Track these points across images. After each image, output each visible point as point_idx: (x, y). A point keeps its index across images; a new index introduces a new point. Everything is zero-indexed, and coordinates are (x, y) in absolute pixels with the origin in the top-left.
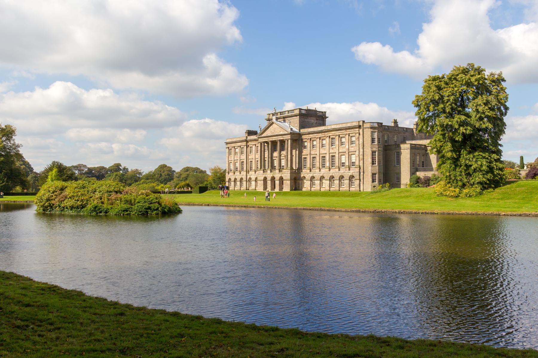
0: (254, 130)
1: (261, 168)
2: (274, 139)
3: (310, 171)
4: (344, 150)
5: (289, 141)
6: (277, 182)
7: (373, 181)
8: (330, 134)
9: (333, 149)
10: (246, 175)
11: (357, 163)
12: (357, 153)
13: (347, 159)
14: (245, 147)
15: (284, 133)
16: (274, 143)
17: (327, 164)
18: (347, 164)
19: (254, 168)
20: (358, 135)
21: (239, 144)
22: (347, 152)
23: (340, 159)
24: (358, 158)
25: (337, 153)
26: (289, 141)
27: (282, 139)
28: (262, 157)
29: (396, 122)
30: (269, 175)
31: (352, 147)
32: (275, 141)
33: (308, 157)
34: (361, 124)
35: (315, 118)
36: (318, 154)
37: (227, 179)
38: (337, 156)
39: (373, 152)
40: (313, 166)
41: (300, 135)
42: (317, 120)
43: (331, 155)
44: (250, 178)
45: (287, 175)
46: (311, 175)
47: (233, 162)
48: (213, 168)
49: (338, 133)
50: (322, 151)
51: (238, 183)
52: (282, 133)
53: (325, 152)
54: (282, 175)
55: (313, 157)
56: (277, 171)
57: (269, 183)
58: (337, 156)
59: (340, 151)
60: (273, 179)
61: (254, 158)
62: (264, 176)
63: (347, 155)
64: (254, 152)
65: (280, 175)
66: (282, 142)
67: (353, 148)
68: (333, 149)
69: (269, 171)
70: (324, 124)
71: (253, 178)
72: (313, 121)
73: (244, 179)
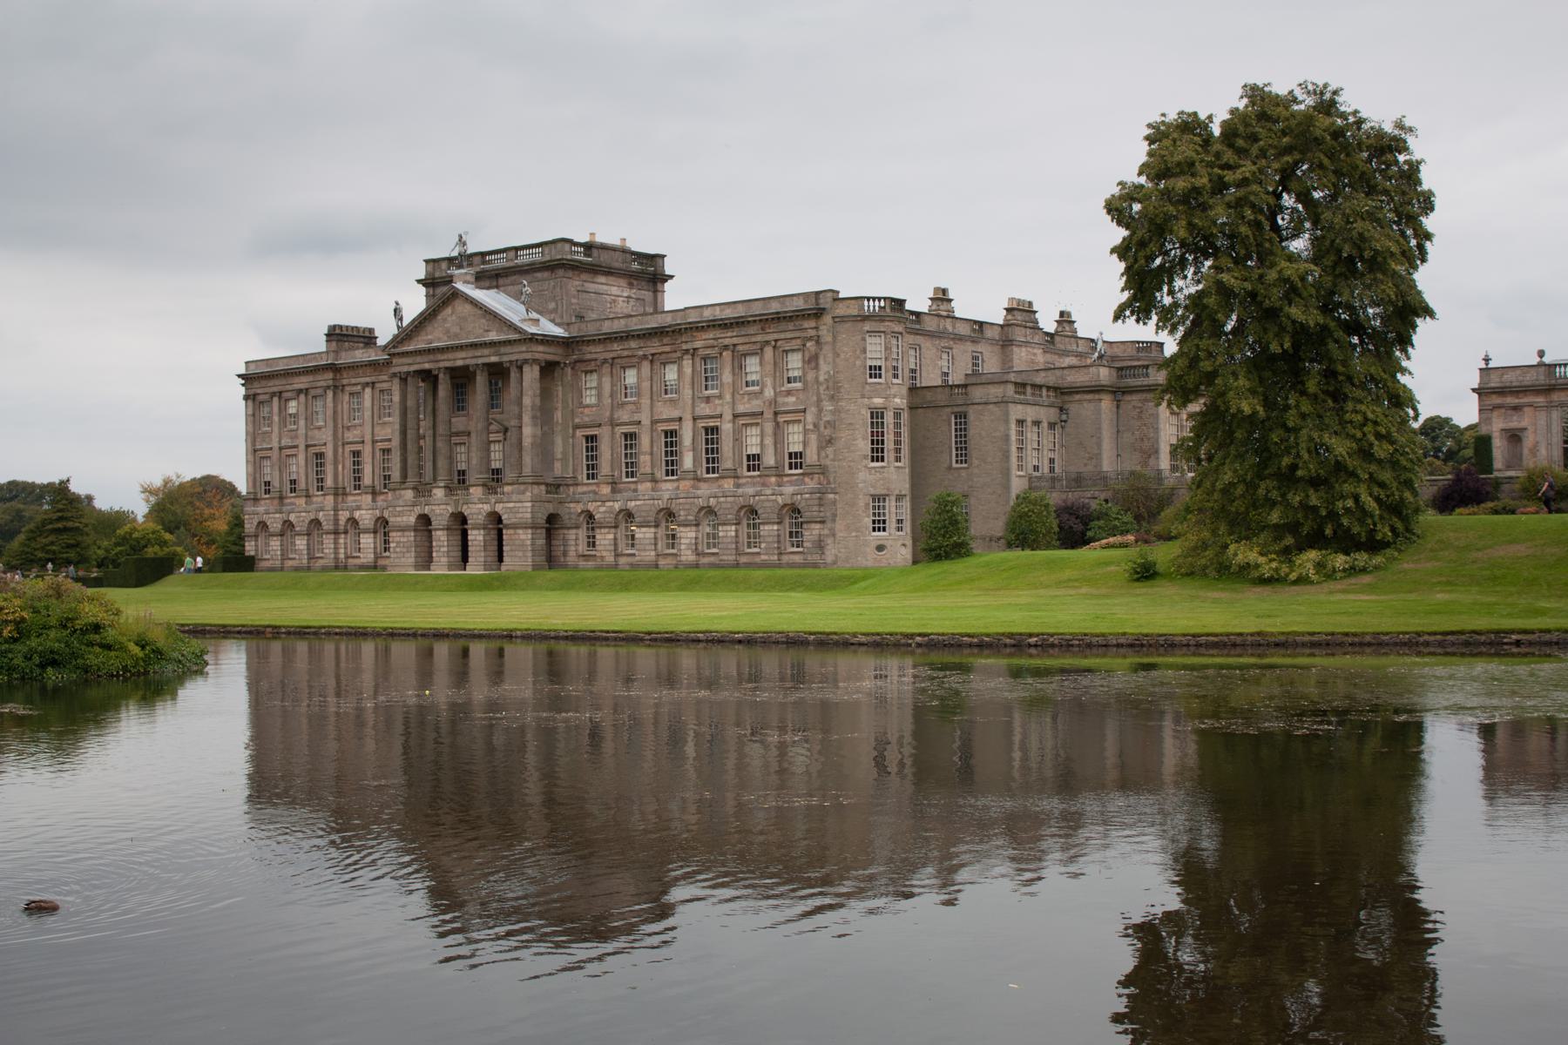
0: (362, 323)
1: (404, 476)
2: (459, 360)
3: (614, 491)
4: (755, 405)
5: (526, 369)
6: (476, 537)
7: (880, 525)
9: (708, 399)
10: (336, 510)
11: (811, 457)
12: (810, 418)
13: (769, 441)
14: (330, 394)
15: (503, 337)
16: (461, 379)
17: (688, 462)
18: (769, 460)
19: (367, 480)
21: (301, 382)
22: (768, 415)
23: (738, 440)
24: (813, 437)
25: (728, 416)
27: (494, 359)
28: (411, 434)
29: (941, 297)
30: (440, 506)
31: (789, 393)
32: (466, 367)
33: (604, 433)
34: (825, 302)
35: (623, 282)
36: (646, 422)
37: (250, 526)
39: (877, 415)
40: (632, 469)
41: (567, 344)
42: (631, 285)
43: (701, 424)
44: (353, 522)
45: (519, 506)
46: (617, 506)
47: (275, 454)
48: (158, 482)
49: (729, 337)
50: (666, 412)
51: (301, 543)
52: (493, 336)
53: (676, 414)
54: (499, 508)
55: (627, 436)
56: (476, 492)
57: (441, 539)
58: (727, 427)
59: (741, 409)
60: (460, 520)
61: (368, 438)
62: (418, 510)
63: (769, 427)
64: (368, 414)
65: (487, 508)
66: (498, 373)
67: (792, 399)
68: (708, 399)
69: (439, 493)
70: (657, 309)
71: (366, 517)
72: (615, 290)
73: (327, 526)
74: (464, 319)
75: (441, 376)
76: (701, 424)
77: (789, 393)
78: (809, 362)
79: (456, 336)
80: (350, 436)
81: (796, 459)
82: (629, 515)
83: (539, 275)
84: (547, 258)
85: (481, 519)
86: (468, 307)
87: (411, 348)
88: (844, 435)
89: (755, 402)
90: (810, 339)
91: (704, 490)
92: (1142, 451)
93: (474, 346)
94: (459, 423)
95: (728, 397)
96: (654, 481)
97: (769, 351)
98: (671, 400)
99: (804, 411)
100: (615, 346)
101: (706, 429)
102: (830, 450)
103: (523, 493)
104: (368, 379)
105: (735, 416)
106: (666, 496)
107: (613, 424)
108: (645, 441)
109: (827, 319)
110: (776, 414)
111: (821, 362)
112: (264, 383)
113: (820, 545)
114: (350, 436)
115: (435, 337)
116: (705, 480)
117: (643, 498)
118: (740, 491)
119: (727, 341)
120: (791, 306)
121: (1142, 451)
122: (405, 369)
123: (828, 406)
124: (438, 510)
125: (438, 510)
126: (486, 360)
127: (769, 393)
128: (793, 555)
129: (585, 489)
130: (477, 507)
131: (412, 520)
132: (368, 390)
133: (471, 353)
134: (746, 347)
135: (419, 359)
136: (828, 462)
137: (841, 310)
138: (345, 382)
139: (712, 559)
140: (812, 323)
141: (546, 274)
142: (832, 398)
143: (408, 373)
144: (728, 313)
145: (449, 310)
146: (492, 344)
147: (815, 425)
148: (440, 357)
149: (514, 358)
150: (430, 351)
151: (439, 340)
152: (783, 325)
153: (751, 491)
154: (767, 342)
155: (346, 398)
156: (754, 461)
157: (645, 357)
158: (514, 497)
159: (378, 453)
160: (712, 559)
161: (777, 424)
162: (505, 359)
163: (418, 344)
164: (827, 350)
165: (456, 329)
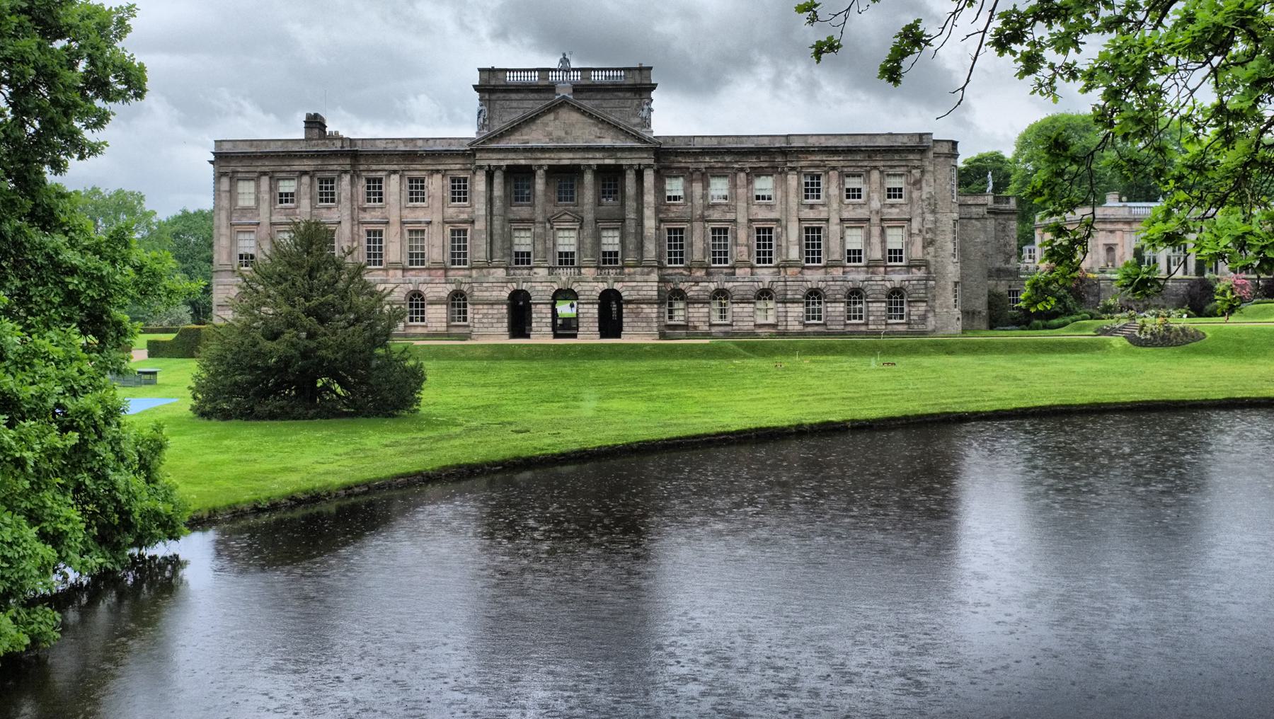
2: (566, 159)
3: (708, 274)
4: (861, 213)
9: (812, 206)
13: (876, 240)
14: (346, 178)
15: (618, 144)
20: (916, 173)
22: (875, 219)
24: (918, 241)
25: (835, 219)
26: (649, 178)
31: (892, 206)
36: (742, 219)
46: (713, 286)
47: (264, 230)
49: (834, 160)
52: (607, 142)
54: (617, 286)
59: (846, 215)
63: (876, 231)
65: (603, 286)
67: (895, 210)
68: (812, 206)
75: (540, 173)
76: (755, 225)
77: (892, 206)
78: (914, 184)
79: (559, 139)
80: (367, 217)
81: (895, 255)
83: (621, 94)
84: (631, 82)
86: (575, 116)
87: (502, 144)
88: (939, 238)
89: (859, 211)
90: (917, 168)
91: (808, 275)
92: (1005, 253)
94: (522, 211)
95: (835, 206)
96: (752, 267)
97: (875, 175)
98: (767, 205)
99: (910, 220)
100: (707, 159)
101: (807, 229)
102: (931, 249)
103: (648, 274)
104: (395, 167)
105: (842, 220)
106: (768, 279)
107: (704, 219)
108: (742, 235)
109: (931, 155)
110: (882, 220)
111: (924, 184)
112: (246, 162)
113: (924, 318)
114: (367, 217)
115: (535, 136)
116: (808, 268)
117: (742, 282)
118: (850, 277)
119: (833, 164)
120: (898, 142)
121: (1005, 253)
122: (494, 163)
123: (929, 217)
124: (539, 287)
125: (539, 287)
126: (600, 162)
127: (876, 204)
128: (898, 325)
129: (670, 271)
130: (540, 283)
131: (505, 294)
132: (395, 178)
133: (578, 155)
134: (851, 169)
135: (511, 155)
136: (928, 258)
137: (938, 149)
138: (362, 168)
139: (816, 328)
140: (918, 157)
141: (628, 95)
142: (933, 212)
143: (499, 167)
144: (832, 143)
145: (551, 116)
147: (920, 231)
148: (539, 155)
149: (636, 162)
150: (526, 150)
151: (538, 140)
152: (889, 156)
153: (862, 276)
154: (875, 168)
155: (364, 182)
156: (854, 255)
157: (742, 170)
158: (638, 278)
159: (406, 234)
160: (816, 328)
161: (883, 230)
162: (623, 162)
163: (514, 142)
164: (928, 176)
165: (563, 134)
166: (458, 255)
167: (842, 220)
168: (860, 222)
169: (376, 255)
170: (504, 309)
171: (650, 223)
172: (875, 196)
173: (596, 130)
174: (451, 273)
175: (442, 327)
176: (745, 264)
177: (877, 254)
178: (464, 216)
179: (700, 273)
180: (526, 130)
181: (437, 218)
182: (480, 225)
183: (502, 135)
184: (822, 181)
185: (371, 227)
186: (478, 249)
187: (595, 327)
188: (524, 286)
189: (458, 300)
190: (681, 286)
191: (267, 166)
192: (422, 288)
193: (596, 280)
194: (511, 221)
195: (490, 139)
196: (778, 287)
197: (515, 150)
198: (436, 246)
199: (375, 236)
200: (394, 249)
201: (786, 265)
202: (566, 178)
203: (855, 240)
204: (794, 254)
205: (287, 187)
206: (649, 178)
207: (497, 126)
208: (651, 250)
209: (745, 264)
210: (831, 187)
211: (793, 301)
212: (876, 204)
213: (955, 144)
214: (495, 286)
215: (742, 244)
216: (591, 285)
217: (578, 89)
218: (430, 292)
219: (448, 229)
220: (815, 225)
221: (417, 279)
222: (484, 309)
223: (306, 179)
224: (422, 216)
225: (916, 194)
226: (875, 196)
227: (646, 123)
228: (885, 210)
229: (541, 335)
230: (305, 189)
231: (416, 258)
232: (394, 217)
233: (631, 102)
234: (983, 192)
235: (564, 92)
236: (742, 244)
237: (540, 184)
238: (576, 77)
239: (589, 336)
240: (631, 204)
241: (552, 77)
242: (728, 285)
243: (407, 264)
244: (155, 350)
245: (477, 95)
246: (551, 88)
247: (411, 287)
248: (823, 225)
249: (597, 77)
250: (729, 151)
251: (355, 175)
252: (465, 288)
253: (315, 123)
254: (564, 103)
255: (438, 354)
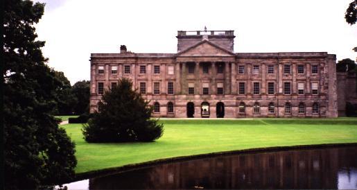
2: (206, 60)
4: (304, 78)
8: (285, 61)
9: (287, 76)
23: (297, 86)
25: (294, 80)
31: (314, 76)
36: (264, 79)
38: (294, 83)
46: (254, 101)
52: (219, 55)
54: (222, 101)
59: (298, 78)
63: (308, 84)
65: (218, 101)
68: (287, 76)
74: (207, 49)
77: (314, 76)
79: (204, 53)
82: (257, 103)
85: (215, 104)
86: (209, 46)
88: (329, 87)
93: (213, 57)
94: (191, 76)
105: (297, 80)
107: (251, 80)
108: (264, 85)
113: (325, 112)
115: (196, 53)
122: (182, 61)
127: (308, 75)
130: (197, 99)
131: (186, 103)
132: (149, 66)
142: (328, 77)
145: (200, 46)
146: (218, 57)
156: (301, 92)
166: (171, 89)
167: (297, 80)
168: (303, 81)
169: (143, 90)
170: (185, 108)
171: (233, 80)
172: (308, 72)
173: (216, 51)
174: (168, 97)
175: (165, 114)
176: (264, 94)
177: (309, 91)
178: (172, 78)
179: (249, 97)
180: (192, 50)
181: (163, 79)
182: (178, 81)
183: (184, 52)
184: (291, 67)
185: (142, 81)
186: (177, 88)
187: (215, 114)
188: (192, 101)
189: (170, 106)
190: (244, 101)
191: (108, 61)
192: (159, 101)
193: (215, 99)
194: (187, 80)
195: (180, 54)
196: (275, 102)
197: (189, 57)
198: (164, 88)
199: (143, 85)
200: (150, 89)
201: (278, 94)
202: (206, 66)
203: (301, 86)
204: (281, 91)
205: (114, 68)
206: (233, 65)
207: (184, 49)
208: (234, 90)
209: (264, 94)
210: (294, 70)
211: (282, 106)
212: (308, 75)
213: (335, 56)
214: (182, 101)
215: (264, 89)
216: (214, 100)
217: (209, 37)
218: (161, 102)
219: (167, 83)
220: (288, 81)
221: (157, 98)
222: (179, 108)
223: (120, 66)
224: (158, 78)
225: (322, 72)
226: (308, 72)
227: (232, 47)
228: (312, 77)
229: (197, 116)
230: (120, 69)
231: (157, 92)
232: (149, 79)
233: (226, 41)
234: (345, 71)
235: (205, 39)
236: (264, 89)
237: (197, 68)
238: (209, 33)
239: (213, 118)
240: (228, 75)
241: (201, 34)
242: (259, 101)
243: (153, 93)
244: (71, 121)
245: (234, 35)
246: (201, 37)
247: (155, 101)
248: (291, 81)
249: (216, 34)
250: (260, 58)
251: (136, 64)
252: (172, 101)
253: (123, 48)
254: (205, 41)
255: (168, 122)
